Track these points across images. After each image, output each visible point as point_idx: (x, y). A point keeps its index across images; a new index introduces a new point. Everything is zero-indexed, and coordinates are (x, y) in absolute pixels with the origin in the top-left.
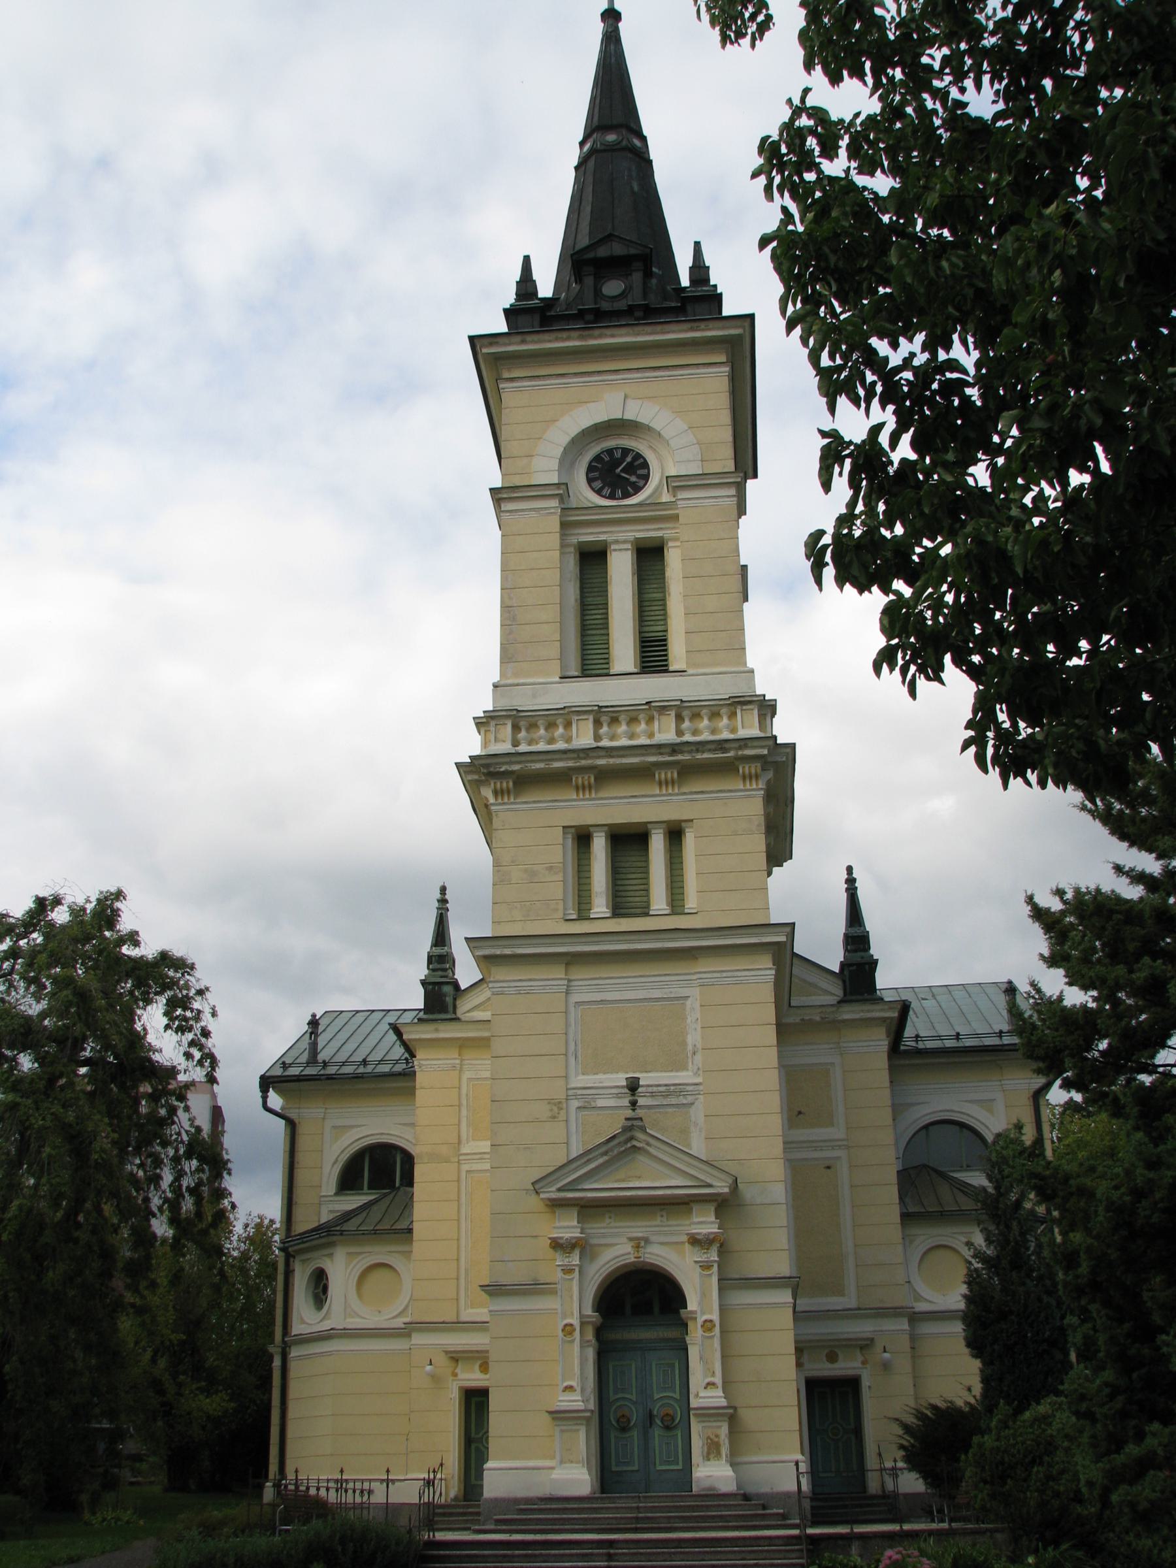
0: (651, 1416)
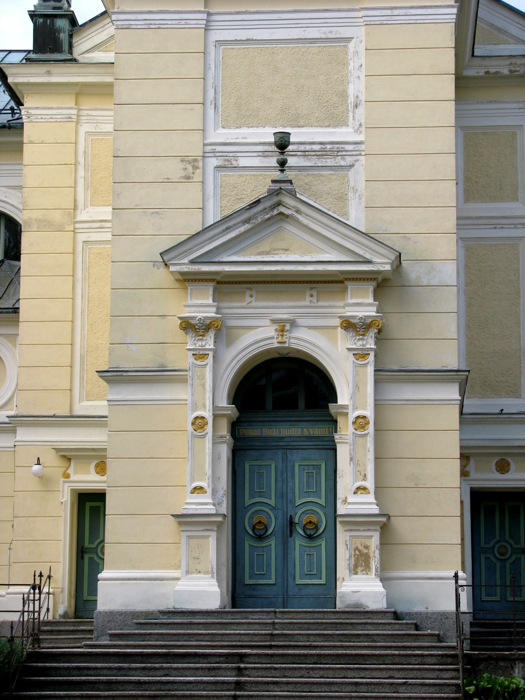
0: (292, 523)
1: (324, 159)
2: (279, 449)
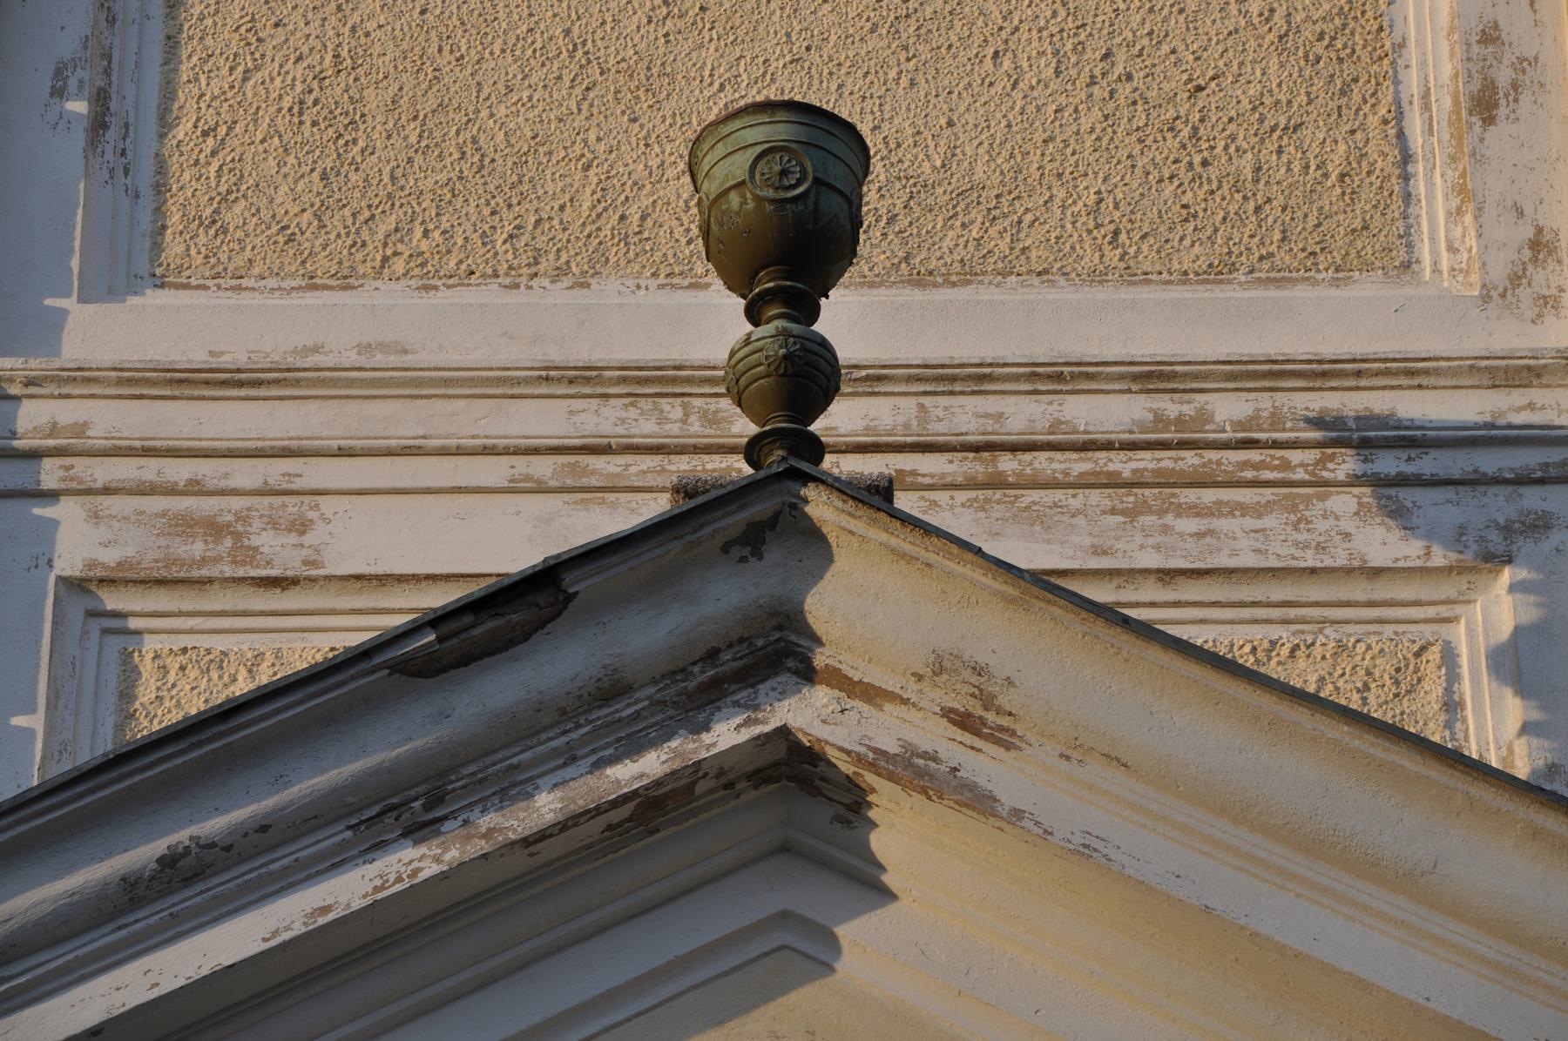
1: (1181, 510)
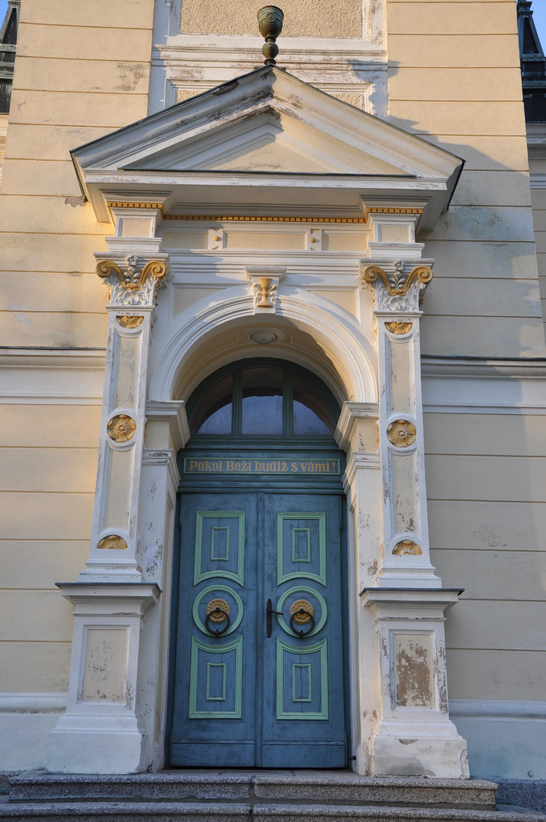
0: (271, 613)
1: (327, 74)
2: (252, 493)
